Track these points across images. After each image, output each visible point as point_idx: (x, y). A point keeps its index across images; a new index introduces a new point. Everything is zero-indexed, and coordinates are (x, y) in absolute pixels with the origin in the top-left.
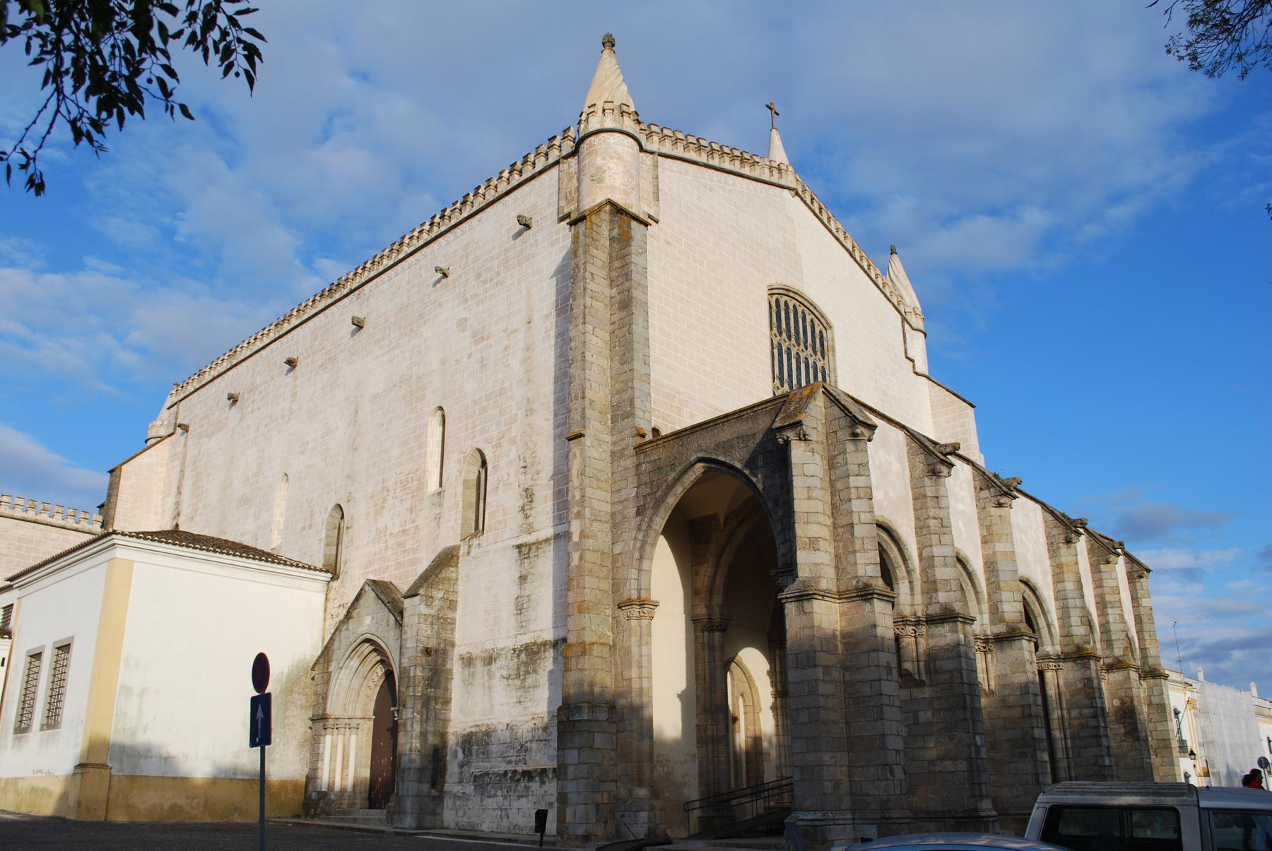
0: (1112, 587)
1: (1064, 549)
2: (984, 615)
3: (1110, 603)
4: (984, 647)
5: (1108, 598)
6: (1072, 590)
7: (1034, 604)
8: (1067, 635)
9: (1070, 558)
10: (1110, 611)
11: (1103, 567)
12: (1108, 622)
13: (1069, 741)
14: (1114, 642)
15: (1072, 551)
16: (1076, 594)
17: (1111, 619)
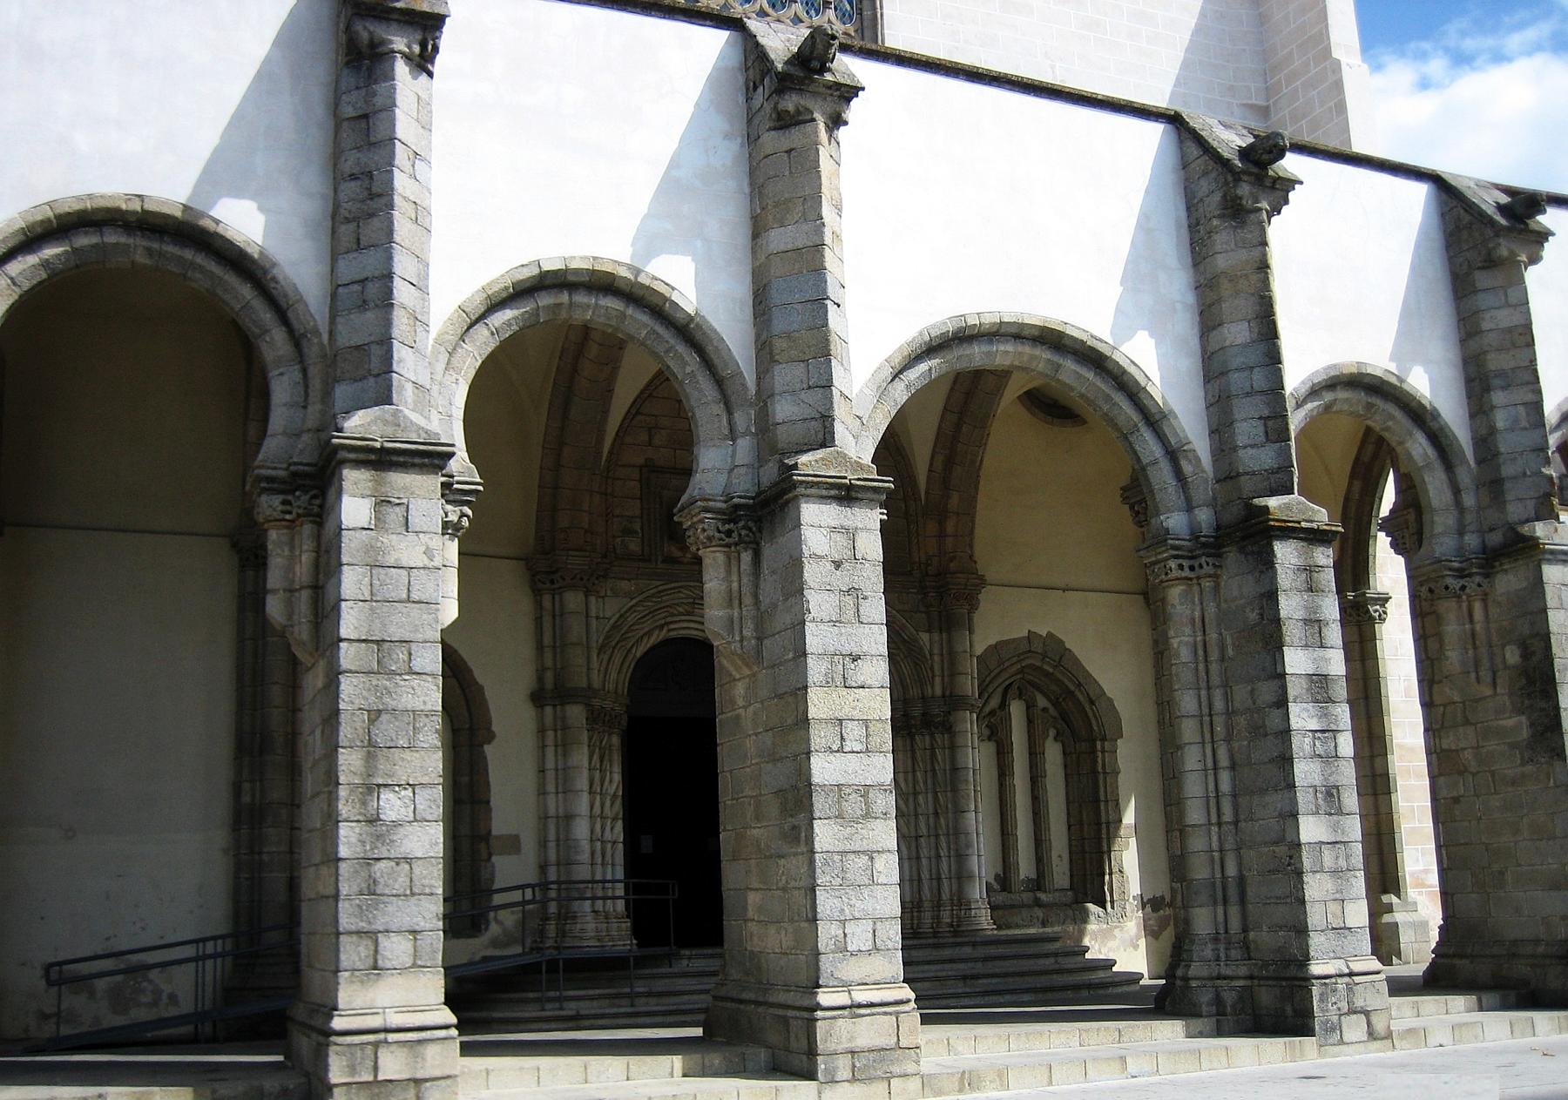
0: (1510, 330)
1: (1223, 238)
2: (740, 441)
3: (1501, 374)
4: (729, 533)
5: (1495, 362)
6: (1245, 346)
7: (1108, 398)
8: (1228, 476)
9: (1243, 255)
10: (1498, 397)
11: (1483, 279)
12: (1493, 430)
13: (1225, 778)
14: (1508, 485)
15: (1248, 234)
16: (1255, 356)
17: (1501, 420)
